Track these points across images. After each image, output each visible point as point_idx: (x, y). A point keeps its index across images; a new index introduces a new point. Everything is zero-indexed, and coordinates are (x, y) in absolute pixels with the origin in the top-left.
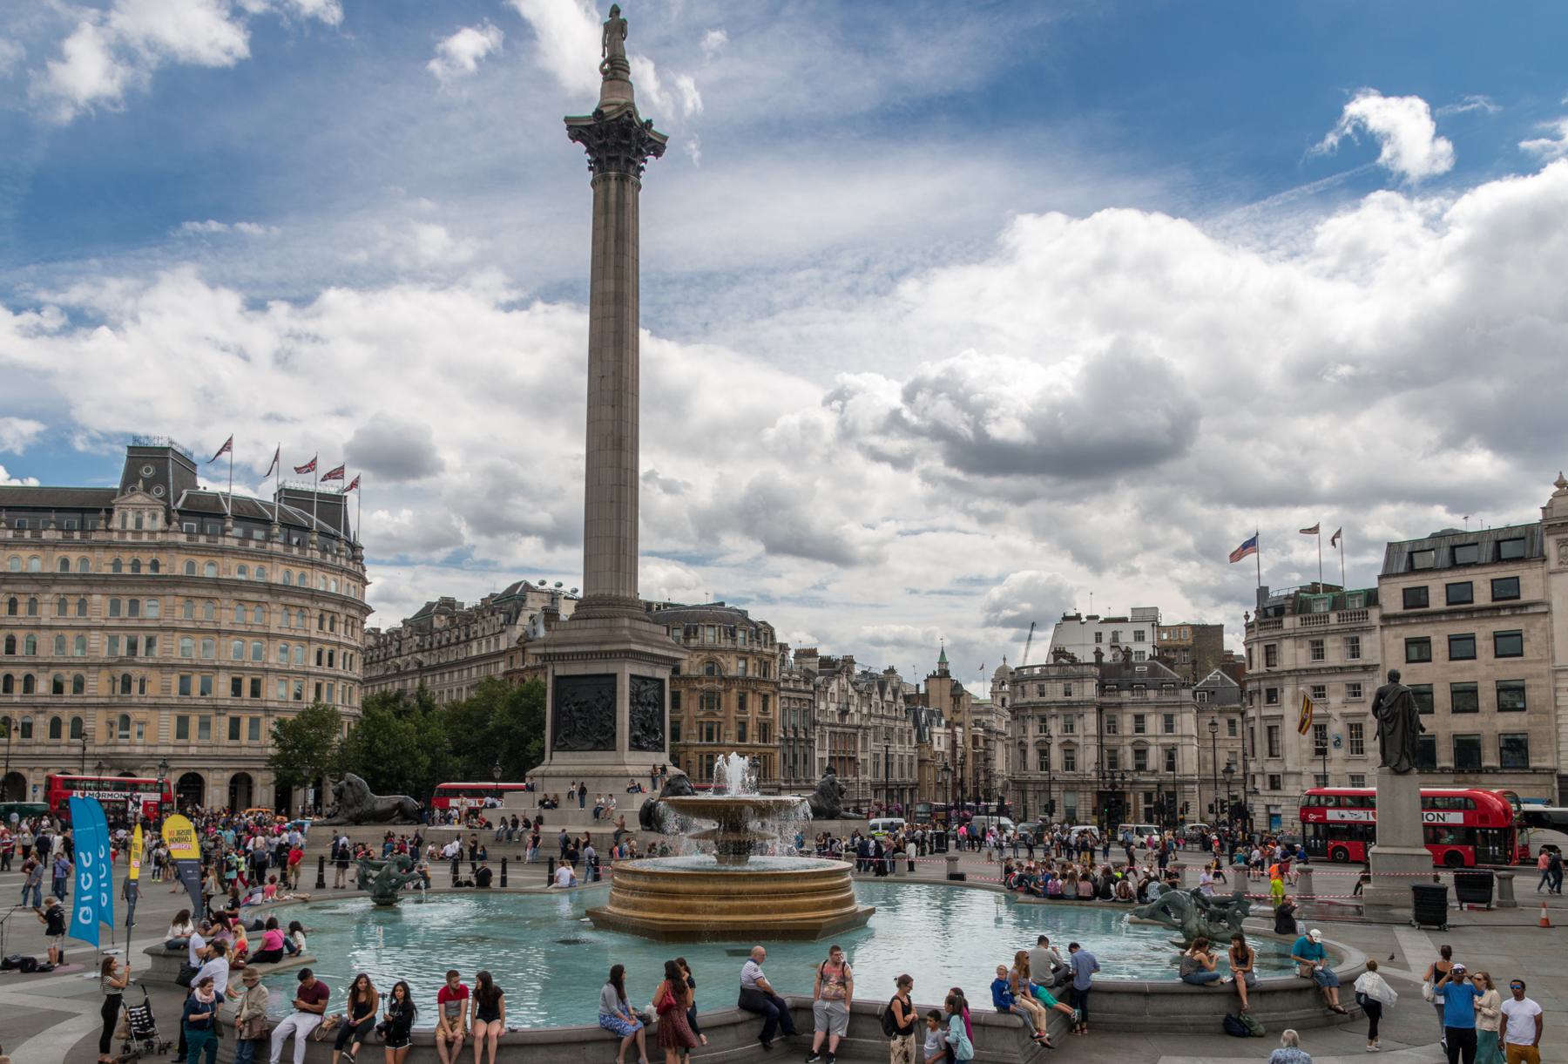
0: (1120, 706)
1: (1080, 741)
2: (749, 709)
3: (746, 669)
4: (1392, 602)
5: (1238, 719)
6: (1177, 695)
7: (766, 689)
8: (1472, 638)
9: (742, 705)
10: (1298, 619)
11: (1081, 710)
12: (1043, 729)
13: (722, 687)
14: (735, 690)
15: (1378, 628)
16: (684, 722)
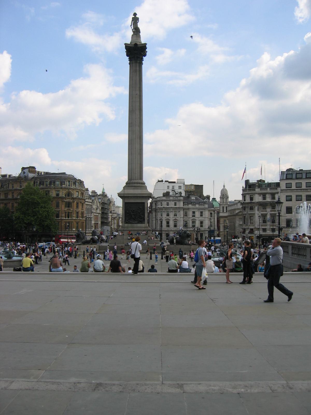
0: (188, 209)
1: (179, 219)
2: (79, 208)
3: (78, 195)
4: (283, 186)
5: (213, 213)
6: (204, 206)
7: (83, 201)
8: (301, 196)
9: (77, 207)
10: (259, 189)
11: (179, 210)
12: (168, 215)
13: (72, 201)
14: (75, 202)
15: (280, 193)
16: (60, 212)
